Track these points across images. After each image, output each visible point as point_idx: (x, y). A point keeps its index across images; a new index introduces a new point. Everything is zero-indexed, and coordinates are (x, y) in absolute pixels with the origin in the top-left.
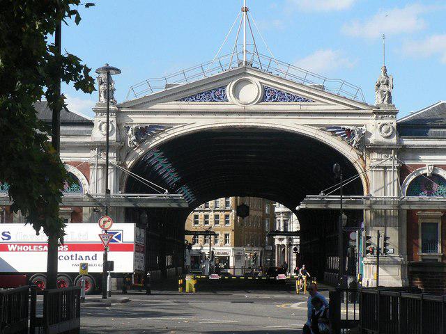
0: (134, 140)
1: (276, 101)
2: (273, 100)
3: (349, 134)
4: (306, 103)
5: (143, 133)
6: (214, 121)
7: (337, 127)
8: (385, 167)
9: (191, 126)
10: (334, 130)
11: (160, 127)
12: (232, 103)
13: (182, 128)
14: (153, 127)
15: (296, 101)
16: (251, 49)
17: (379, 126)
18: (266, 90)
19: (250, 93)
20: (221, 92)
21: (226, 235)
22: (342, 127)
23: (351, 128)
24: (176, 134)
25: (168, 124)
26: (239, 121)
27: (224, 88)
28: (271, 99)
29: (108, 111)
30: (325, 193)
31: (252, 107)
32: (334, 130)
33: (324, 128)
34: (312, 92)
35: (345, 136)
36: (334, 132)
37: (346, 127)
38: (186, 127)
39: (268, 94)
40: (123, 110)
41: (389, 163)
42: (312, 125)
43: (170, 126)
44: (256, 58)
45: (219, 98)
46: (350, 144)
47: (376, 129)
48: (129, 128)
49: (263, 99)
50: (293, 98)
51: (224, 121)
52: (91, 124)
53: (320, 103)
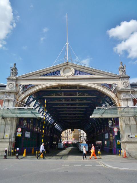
0: (22, 90)
3: (110, 86)
4: (92, 75)
5: (26, 87)
7: (106, 84)
8: (127, 99)
9: (45, 85)
10: (104, 86)
11: (33, 85)
12: (63, 75)
13: (42, 86)
14: (30, 85)
17: (123, 83)
18: (76, 71)
19: (70, 73)
21: (71, 138)
22: (107, 84)
23: (111, 84)
28: (78, 74)
32: (104, 86)
33: (98, 84)
35: (108, 87)
36: (104, 86)
37: (109, 84)
38: (43, 85)
39: (77, 72)
40: (18, 79)
41: (128, 97)
42: (95, 83)
43: (37, 85)
45: (57, 74)
46: (111, 91)
48: (20, 86)
49: (75, 74)
50: (86, 73)
51: (59, 83)
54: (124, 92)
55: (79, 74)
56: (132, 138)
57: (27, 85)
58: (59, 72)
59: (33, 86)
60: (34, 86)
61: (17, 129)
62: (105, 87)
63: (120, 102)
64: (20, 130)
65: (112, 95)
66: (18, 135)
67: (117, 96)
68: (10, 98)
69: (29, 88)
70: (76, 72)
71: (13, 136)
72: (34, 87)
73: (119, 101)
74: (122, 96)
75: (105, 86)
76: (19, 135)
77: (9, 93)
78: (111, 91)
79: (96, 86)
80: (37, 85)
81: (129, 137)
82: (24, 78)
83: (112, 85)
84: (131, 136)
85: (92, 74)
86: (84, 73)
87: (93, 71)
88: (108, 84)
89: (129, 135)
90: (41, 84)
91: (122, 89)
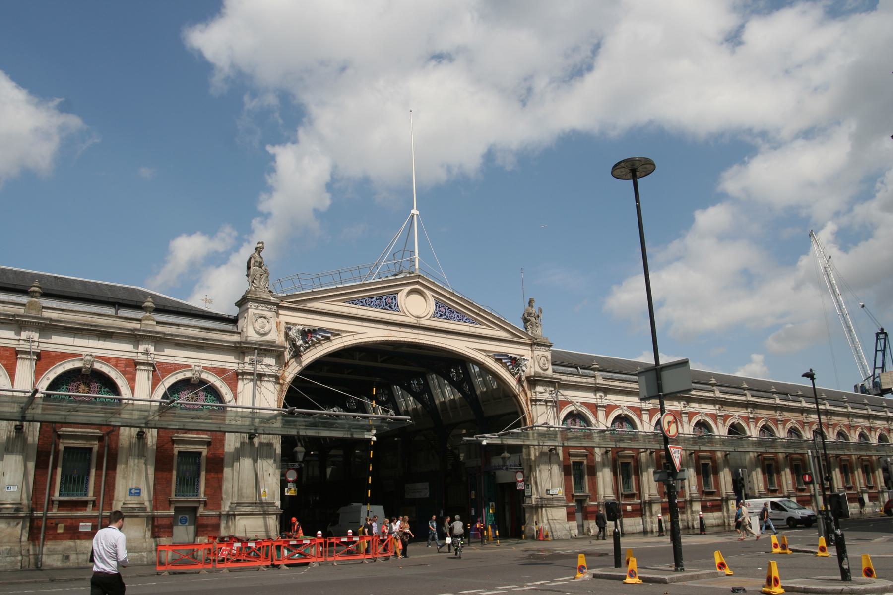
1: (446, 319)
2: (443, 317)
6: (386, 333)
7: (505, 355)
8: (546, 401)
11: (328, 333)
13: (351, 338)
14: (321, 330)
15: (465, 322)
20: (392, 299)
22: (509, 355)
23: (518, 357)
24: (346, 344)
25: (336, 330)
26: (413, 336)
28: (441, 315)
31: (425, 322)
32: (499, 358)
34: (481, 313)
37: (514, 356)
38: (357, 337)
39: (444, 310)
43: (337, 333)
45: (390, 307)
50: (462, 318)
51: (397, 334)
53: (485, 327)
54: (541, 383)
55: (445, 315)
56: (552, 495)
57: (314, 330)
58: (395, 299)
59: (328, 335)
60: (330, 335)
62: (501, 363)
63: (530, 407)
64: (292, 476)
66: (287, 493)
68: (260, 369)
69: (317, 339)
70: (437, 309)
72: (328, 338)
73: (529, 403)
75: (503, 361)
77: (266, 349)
78: (513, 375)
79: (483, 357)
80: (337, 333)
81: (547, 494)
83: (519, 359)
84: (551, 492)
85: (474, 321)
86: (455, 313)
87: (478, 315)
88: (511, 357)
89: (547, 490)
90: (349, 332)
91: (537, 375)
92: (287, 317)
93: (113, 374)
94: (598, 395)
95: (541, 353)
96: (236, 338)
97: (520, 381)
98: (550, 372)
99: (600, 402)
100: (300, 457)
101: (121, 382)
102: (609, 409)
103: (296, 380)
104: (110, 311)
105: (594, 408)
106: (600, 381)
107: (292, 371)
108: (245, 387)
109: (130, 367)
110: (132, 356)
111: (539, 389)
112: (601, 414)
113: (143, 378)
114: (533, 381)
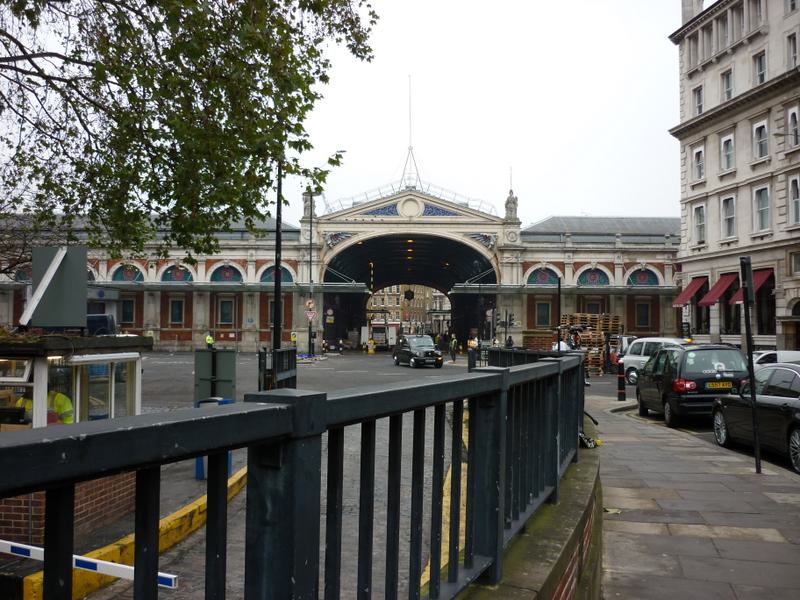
3: (486, 238)
5: (336, 237)
6: (387, 230)
7: (479, 234)
8: (512, 263)
16: (414, 176)
18: (426, 206)
27: (395, 206)
29: (311, 222)
30: (470, 282)
31: (415, 219)
32: (474, 236)
33: (466, 234)
41: (514, 260)
43: (355, 234)
44: (418, 183)
47: (503, 236)
50: (445, 213)
52: (298, 232)
59: (348, 235)
61: (325, 310)
64: (330, 312)
65: (489, 255)
66: (328, 321)
67: (495, 255)
71: (321, 322)
74: (507, 257)
76: (330, 320)
77: (310, 248)
80: (355, 234)
82: (330, 220)
85: (455, 214)
91: (506, 246)
92: (324, 228)
93: (238, 267)
94: (567, 254)
95: (510, 230)
96: (296, 243)
97: (491, 249)
98: (519, 242)
99: (566, 261)
100: (337, 302)
101: (241, 270)
102: (577, 265)
103: (331, 264)
104: (239, 235)
105: (561, 266)
106: (569, 245)
107: (327, 259)
108: (303, 270)
109: (244, 263)
110: (245, 258)
111: (506, 255)
112: (568, 271)
113: (251, 268)
114: (502, 250)
